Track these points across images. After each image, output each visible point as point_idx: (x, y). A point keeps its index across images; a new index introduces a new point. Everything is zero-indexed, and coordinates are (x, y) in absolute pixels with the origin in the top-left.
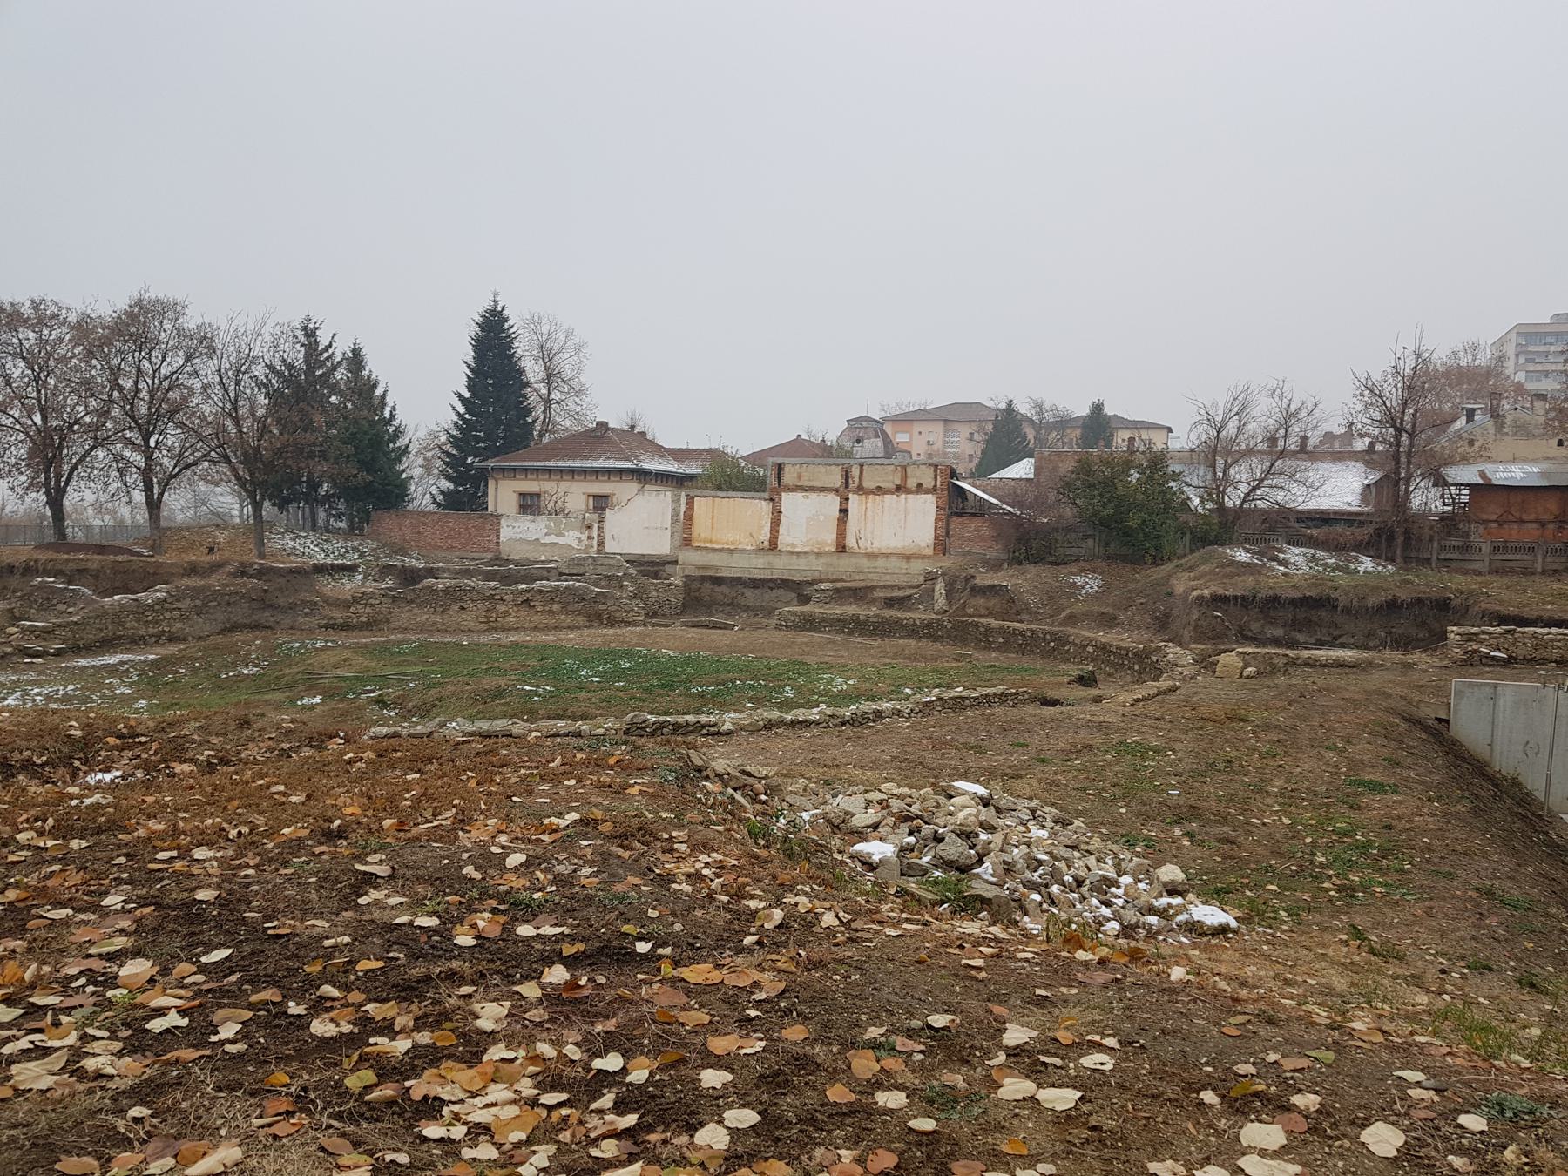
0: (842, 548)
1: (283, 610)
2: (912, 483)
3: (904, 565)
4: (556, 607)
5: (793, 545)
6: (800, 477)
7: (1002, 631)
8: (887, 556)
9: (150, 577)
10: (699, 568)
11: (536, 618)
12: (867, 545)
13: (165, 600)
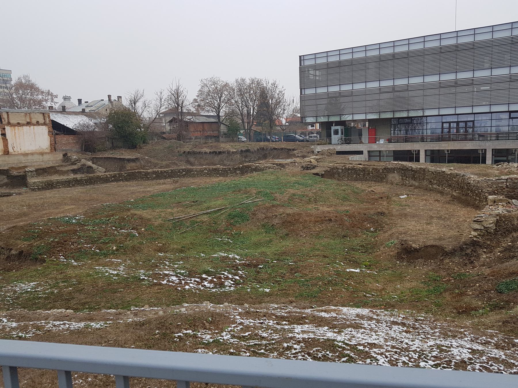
2: (34, 121)
3: (41, 157)
7: (154, 172)
8: (32, 154)
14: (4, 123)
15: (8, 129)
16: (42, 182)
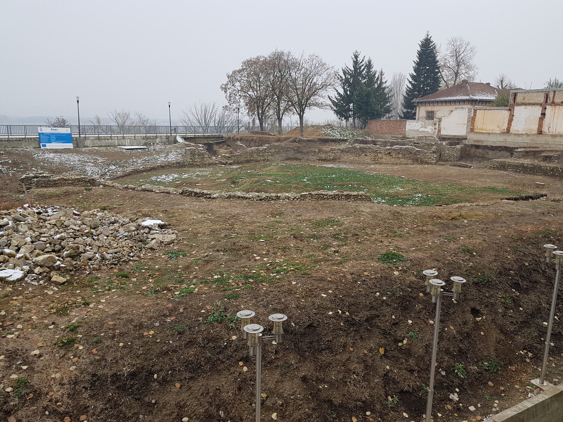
0: (540, 132)
4: (400, 156)
5: (518, 131)
6: (524, 99)
9: (261, 142)
10: (475, 141)
11: (393, 160)
12: (553, 131)
14: (549, 102)
15: (549, 110)
16: (497, 162)
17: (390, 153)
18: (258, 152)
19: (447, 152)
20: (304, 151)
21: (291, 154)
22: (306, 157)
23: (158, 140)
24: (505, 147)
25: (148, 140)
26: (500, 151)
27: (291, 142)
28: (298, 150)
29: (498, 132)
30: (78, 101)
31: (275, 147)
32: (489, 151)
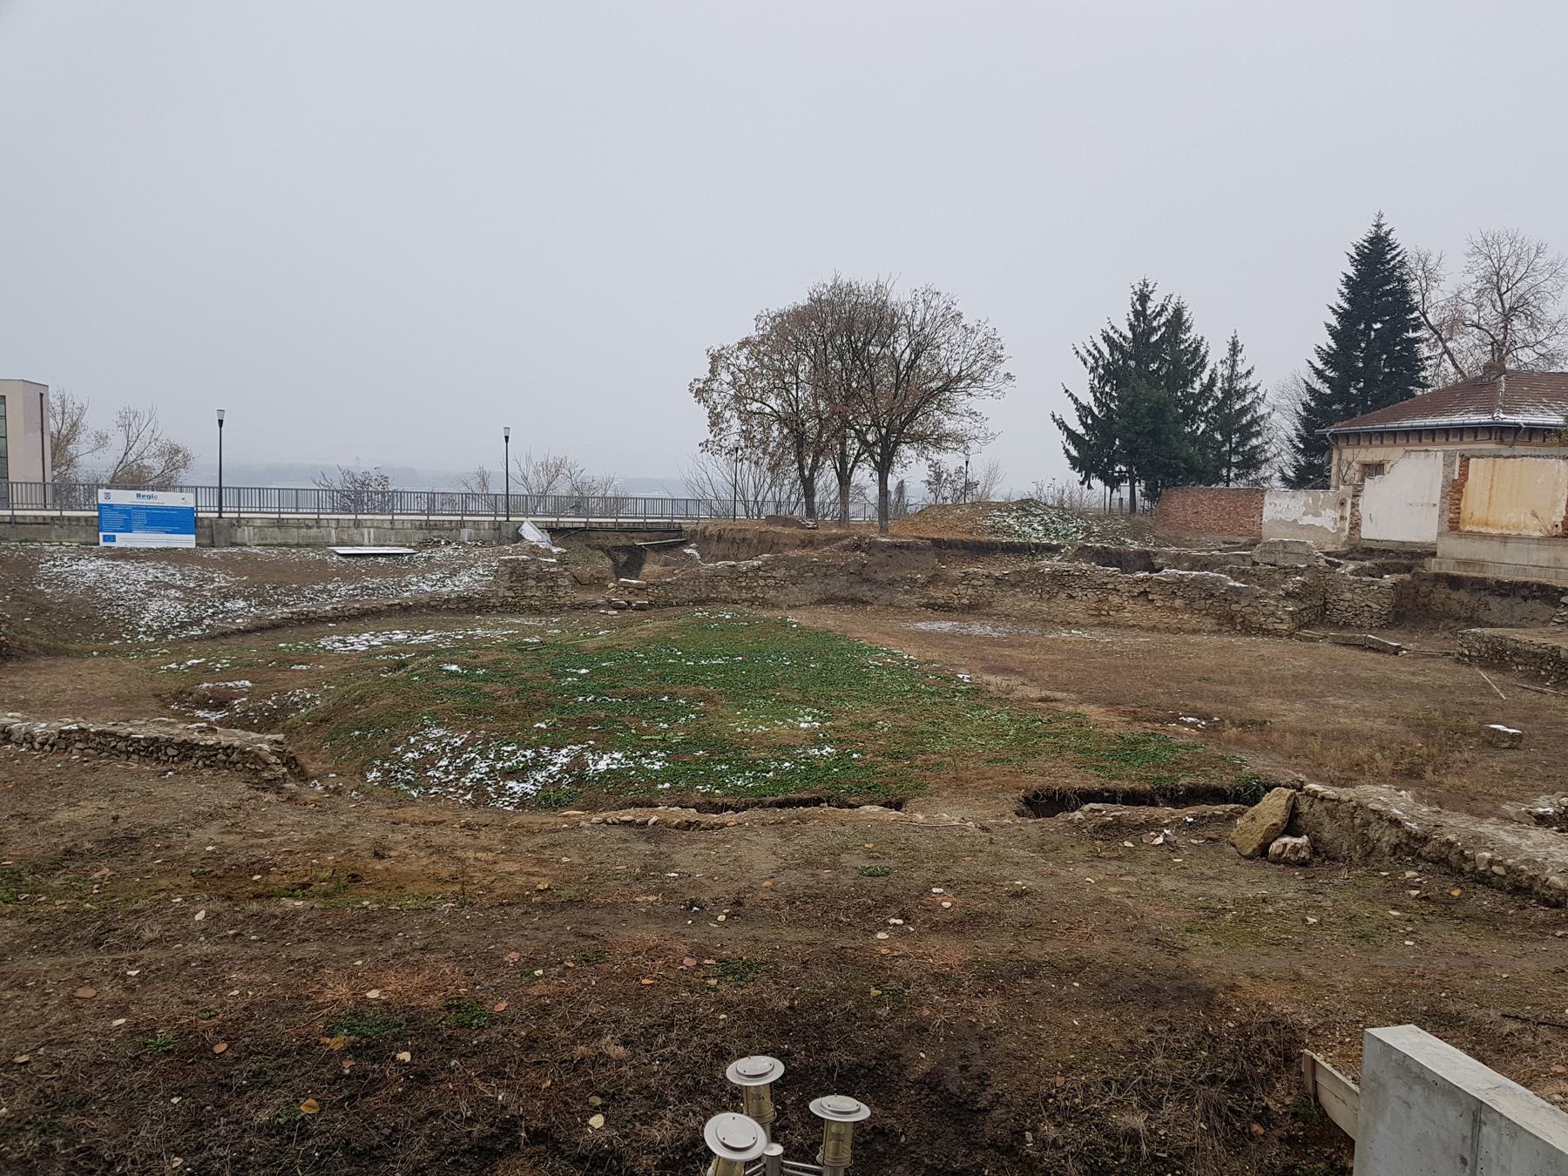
1: (882, 585)
4: (1178, 603)
11: (1155, 615)
13: (759, 568)
16: (1480, 638)
17: (1145, 593)
18: (734, 576)
19: (1348, 595)
20: (880, 576)
21: (838, 586)
22: (886, 597)
23: (465, 534)
24: (1543, 588)
25: (435, 533)
26: (1525, 599)
27: (845, 548)
28: (861, 575)
29: (1537, 534)
30: (221, 422)
31: (790, 563)
32: (1490, 599)
